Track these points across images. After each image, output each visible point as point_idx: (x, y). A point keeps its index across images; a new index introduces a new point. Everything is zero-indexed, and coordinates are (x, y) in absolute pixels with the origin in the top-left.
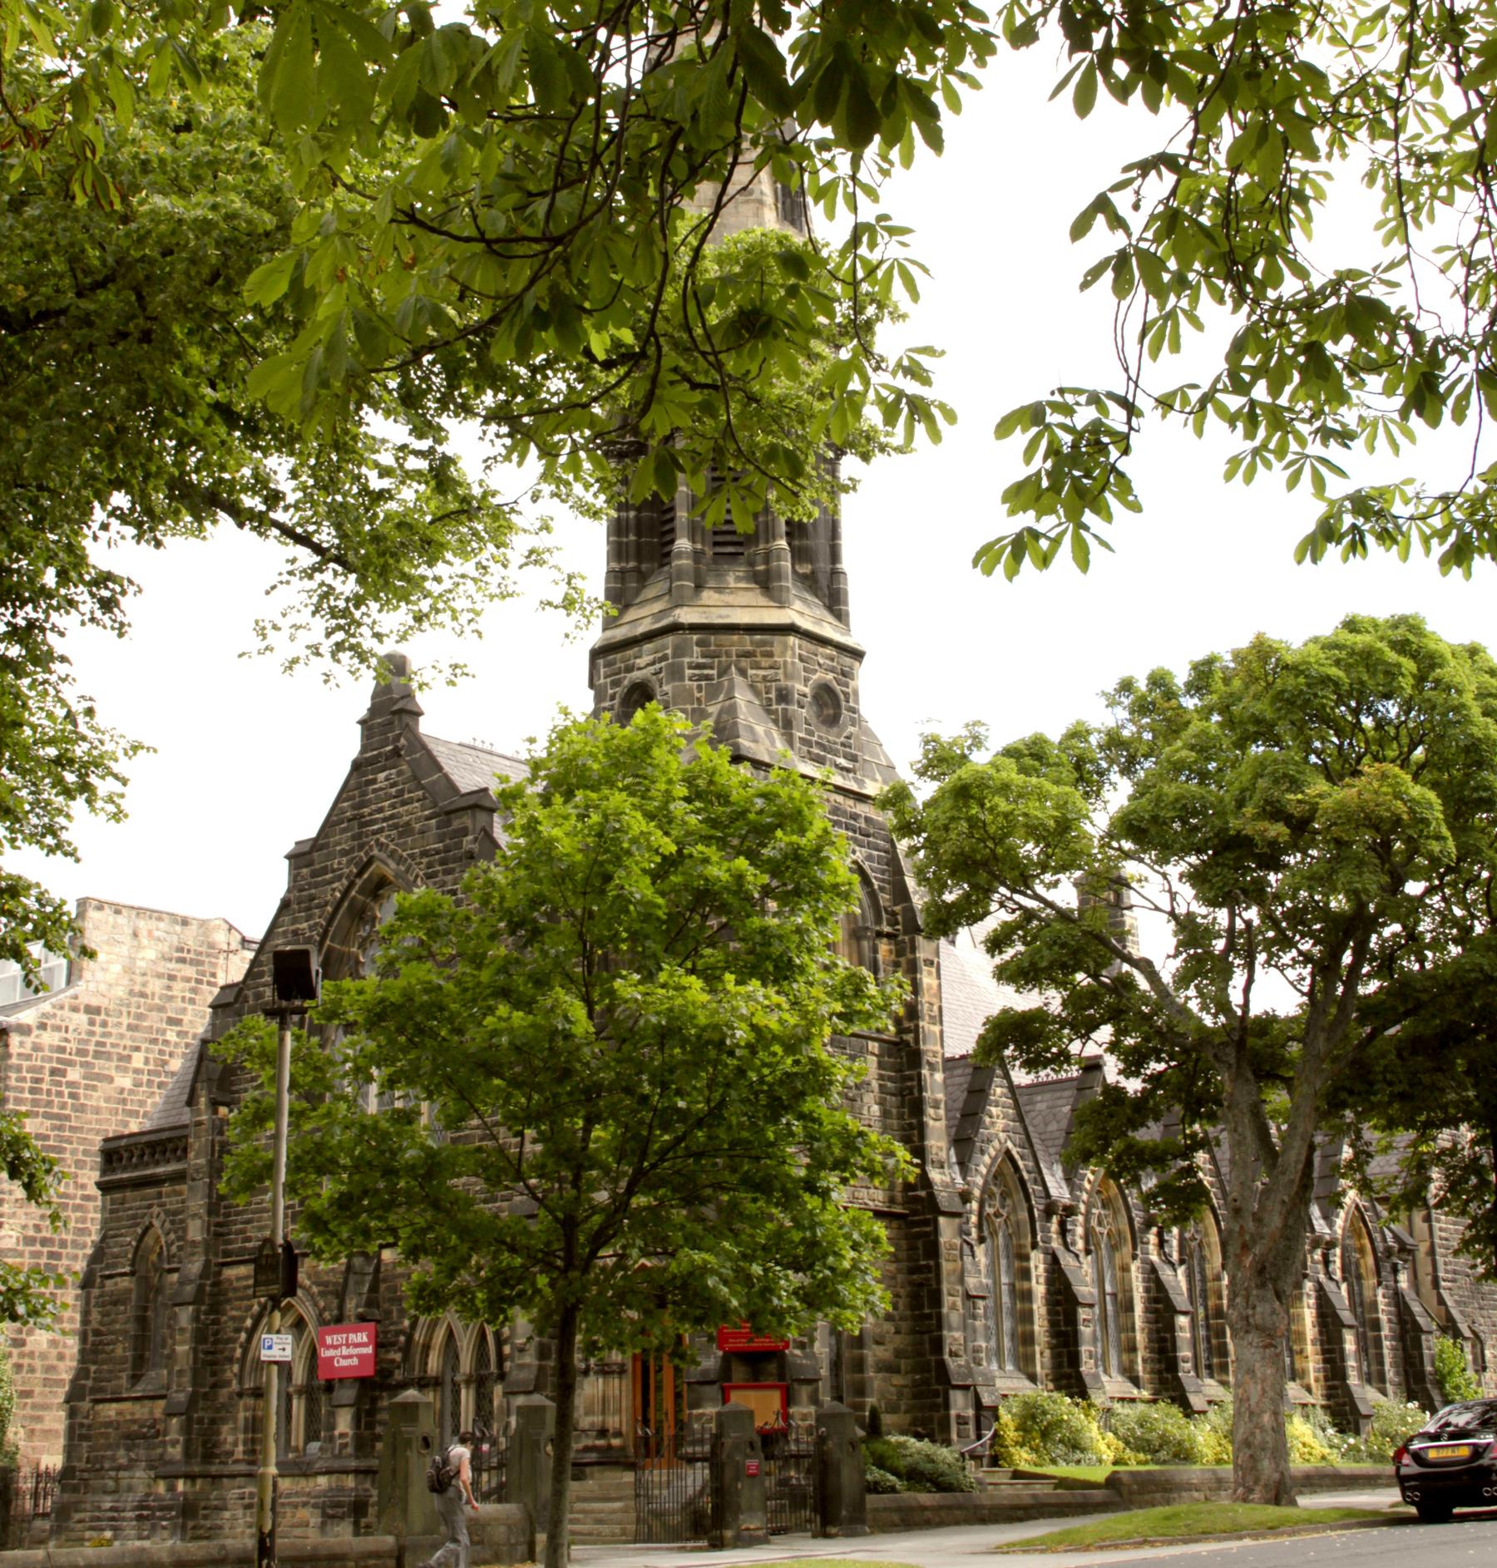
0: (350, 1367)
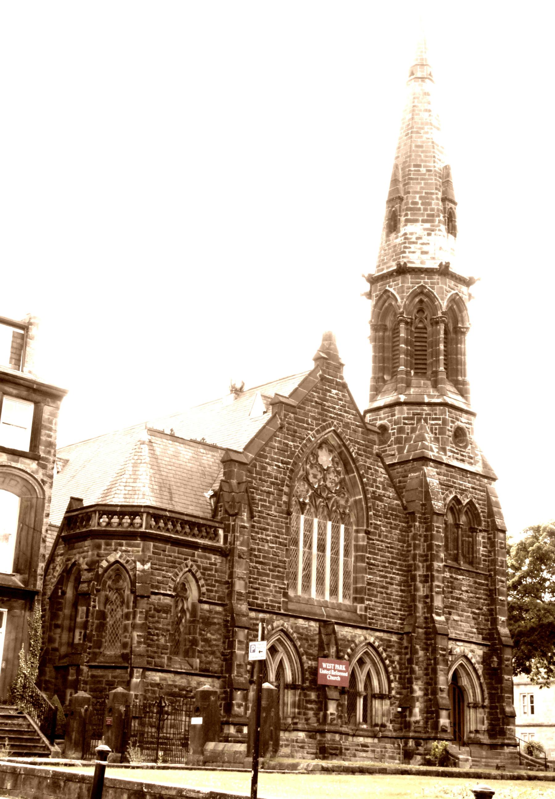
0: (335, 681)
